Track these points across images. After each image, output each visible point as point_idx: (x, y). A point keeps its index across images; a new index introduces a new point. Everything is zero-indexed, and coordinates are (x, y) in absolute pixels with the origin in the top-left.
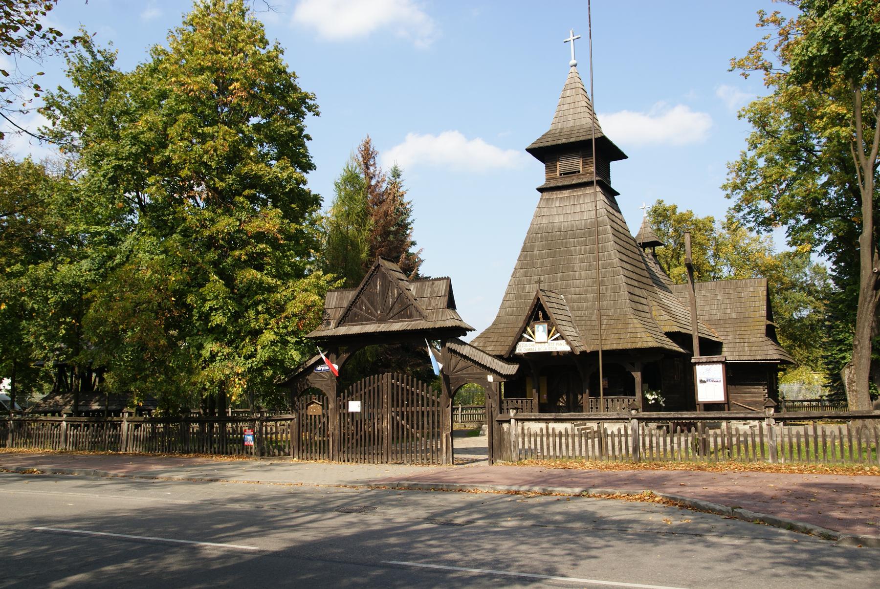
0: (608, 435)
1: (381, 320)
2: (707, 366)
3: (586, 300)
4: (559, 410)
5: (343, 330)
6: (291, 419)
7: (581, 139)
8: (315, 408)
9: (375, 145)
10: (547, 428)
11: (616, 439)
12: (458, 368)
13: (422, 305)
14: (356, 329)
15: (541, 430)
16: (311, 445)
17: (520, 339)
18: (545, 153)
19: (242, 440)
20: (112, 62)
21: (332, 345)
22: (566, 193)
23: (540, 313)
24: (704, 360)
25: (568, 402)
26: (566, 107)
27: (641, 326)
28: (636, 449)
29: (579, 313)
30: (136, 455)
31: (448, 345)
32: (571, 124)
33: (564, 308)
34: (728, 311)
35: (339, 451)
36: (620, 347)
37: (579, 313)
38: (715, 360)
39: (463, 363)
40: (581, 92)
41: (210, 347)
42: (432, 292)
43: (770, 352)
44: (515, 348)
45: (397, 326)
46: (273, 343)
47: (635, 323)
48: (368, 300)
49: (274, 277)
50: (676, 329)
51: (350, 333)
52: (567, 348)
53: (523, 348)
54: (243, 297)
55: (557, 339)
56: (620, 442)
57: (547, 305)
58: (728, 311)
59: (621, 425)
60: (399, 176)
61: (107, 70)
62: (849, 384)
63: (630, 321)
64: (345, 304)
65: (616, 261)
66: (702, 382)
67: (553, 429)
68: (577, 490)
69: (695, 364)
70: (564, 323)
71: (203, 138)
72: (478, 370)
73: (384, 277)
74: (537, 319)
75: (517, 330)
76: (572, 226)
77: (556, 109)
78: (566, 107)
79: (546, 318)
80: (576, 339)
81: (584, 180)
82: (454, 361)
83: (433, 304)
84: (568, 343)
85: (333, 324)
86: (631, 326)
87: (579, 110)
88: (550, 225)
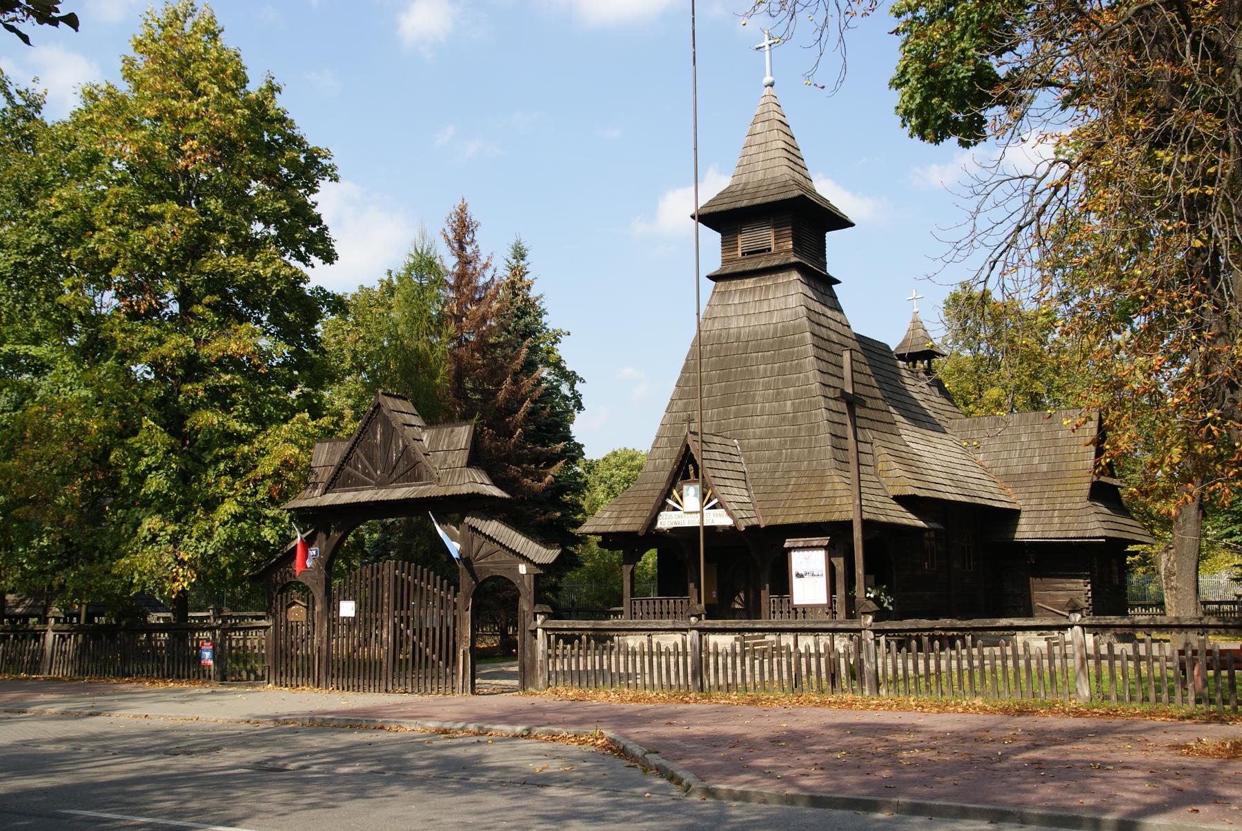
1: (381, 485)
3: (769, 447)
4: (733, 614)
5: (332, 499)
6: (266, 628)
7: (770, 199)
8: (298, 611)
9: (474, 214)
10: (650, 642)
11: (672, 659)
13: (434, 463)
15: (676, 645)
16: (288, 665)
17: (663, 506)
18: (723, 219)
19: (199, 658)
20: (38, 108)
22: (749, 283)
23: (691, 467)
24: (801, 544)
25: (746, 603)
26: (754, 149)
27: (843, 486)
29: (757, 467)
30: (53, 679)
31: (467, 519)
32: (760, 176)
33: (736, 459)
34: (1036, 460)
35: (327, 674)
36: (809, 520)
37: (757, 467)
38: (815, 544)
39: (487, 547)
40: (778, 125)
41: (151, 523)
43: (1091, 526)
44: (654, 520)
46: (237, 518)
49: (248, 421)
50: (910, 491)
51: (338, 502)
52: (728, 522)
53: (667, 521)
54: (193, 454)
55: (714, 507)
58: (1036, 460)
59: (678, 637)
60: (523, 257)
61: (30, 118)
62: (1167, 577)
64: (337, 460)
66: (799, 576)
67: (659, 645)
68: (519, 729)
70: (728, 482)
71: (149, 219)
73: (387, 423)
74: (686, 477)
75: (657, 493)
76: (756, 334)
77: (740, 152)
78: (754, 149)
80: (744, 507)
82: (476, 544)
83: (449, 461)
84: (730, 514)
86: (829, 486)
87: (771, 154)
88: (724, 333)
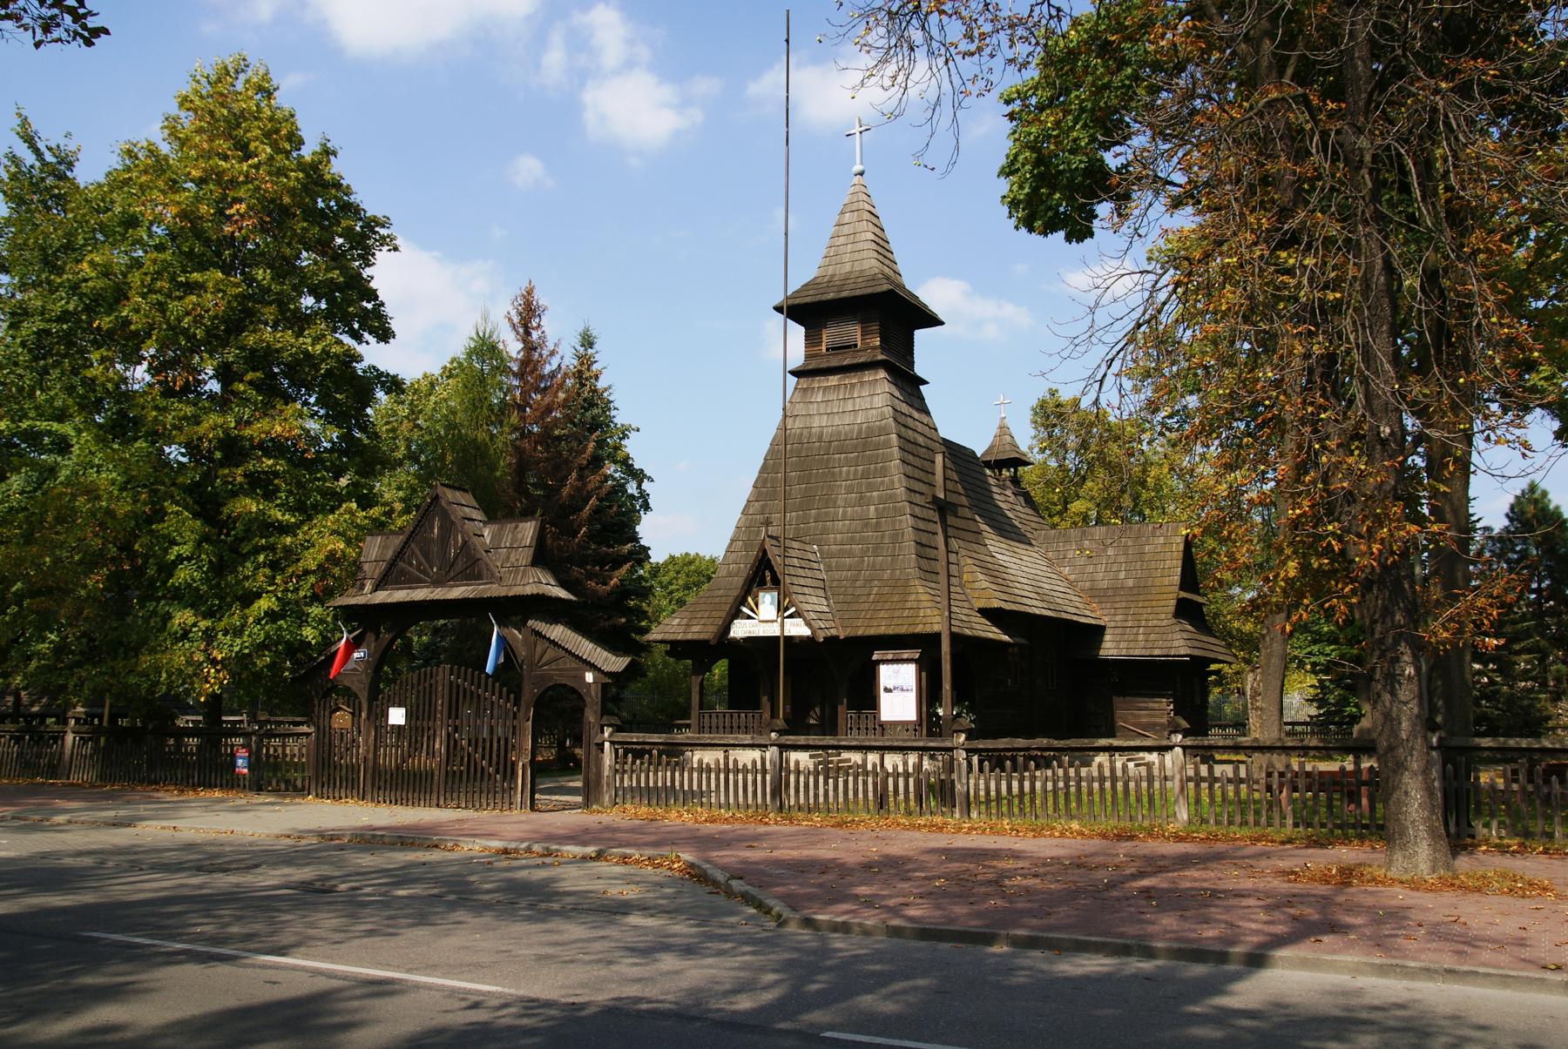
0: (888, 775)
1: (437, 583)
2: (895, 666)
3: (850, 554)
4: (807, 730)
5: (382, 597)
6: (308, 735)
7: (858, 293)
8: (342, 717)
9: (540, 298)
10: (727, 758)
11: (750, 777)
12: (545, 659)
13: (496, 561)
14: (400, 595)
16: (329, 774)
17: (736, 614)
18: (807, 311)
19: (234, 765)
20: (70, 165)
21: (365, 619)
22: (833, 380)
23: (767, 573)
24: (890, 657)
25: (821, 718)
26: (842, 240)
27: (927, 597)
28: (776, 792)
29: (837, 575)
30: (72, 785)
31: (530, 623)
32: (848, 268)
33: (815, 566)
34: (1122, 575)
35: (373, 786)
36: (890, 631)
37: (837, 575)
38: (905, 656)
39: (551, 653)
40: (867, 216)
41: (183, 617)
42: (514, 540)
43: (1176, 643)
44: (727, 629)
45: (457, 592)
46: (272, 616)
47: (921, 593)
48: (421, 550)
49: (291, 510)
50: (996, 604)
51: (390, 600)
52: (807, 632)
53: (740, 630)
54: (230, 546)
55: (791, 616)
56: (755, 782)
57: (777, 562)
58: (1122, 575)
59: (756, 754)
60: (591, 345)
61: (62, 177)
62: (1252, 697)
63: (913, 590)
64: (390, 554)
65: (901, 491)
66: (887, 690)
67: (736, 761)
68: (591, 850)
69: (879, 662)
70: (806, 590)
71: (190, 288)
72: (572, 664)
73: (445, 516)
74: (762, 584)
75: (731, 600)
76: (839, 433)
77: (827, 242)
78: (842, 240)
79: (776, 582)
80: (822, 616)
81: (862, 360)
82: (539, 649)
83: (512, 559)
84: (808, 624)
85: (368, 587)
86: (913, 597)
87: (860, 246)
88: (805, 432)
